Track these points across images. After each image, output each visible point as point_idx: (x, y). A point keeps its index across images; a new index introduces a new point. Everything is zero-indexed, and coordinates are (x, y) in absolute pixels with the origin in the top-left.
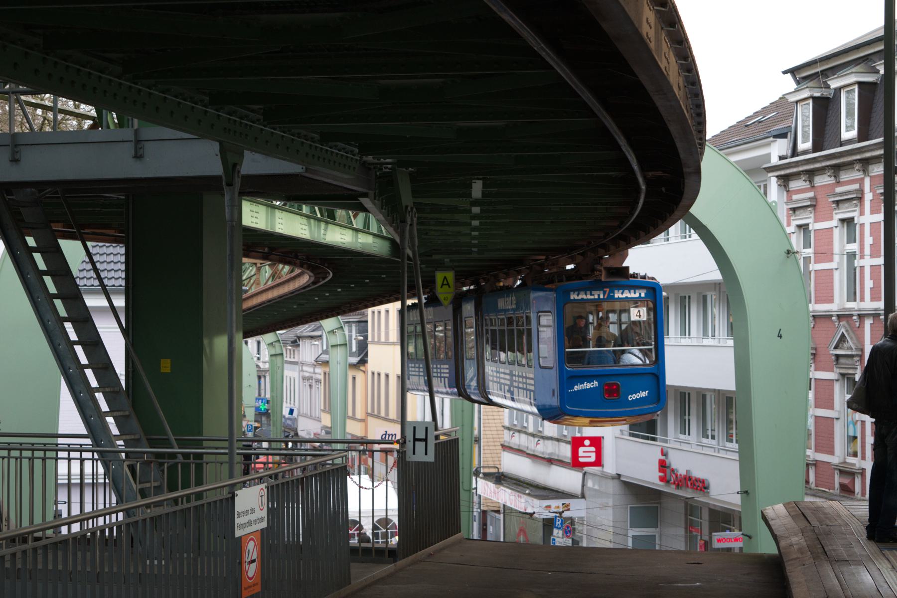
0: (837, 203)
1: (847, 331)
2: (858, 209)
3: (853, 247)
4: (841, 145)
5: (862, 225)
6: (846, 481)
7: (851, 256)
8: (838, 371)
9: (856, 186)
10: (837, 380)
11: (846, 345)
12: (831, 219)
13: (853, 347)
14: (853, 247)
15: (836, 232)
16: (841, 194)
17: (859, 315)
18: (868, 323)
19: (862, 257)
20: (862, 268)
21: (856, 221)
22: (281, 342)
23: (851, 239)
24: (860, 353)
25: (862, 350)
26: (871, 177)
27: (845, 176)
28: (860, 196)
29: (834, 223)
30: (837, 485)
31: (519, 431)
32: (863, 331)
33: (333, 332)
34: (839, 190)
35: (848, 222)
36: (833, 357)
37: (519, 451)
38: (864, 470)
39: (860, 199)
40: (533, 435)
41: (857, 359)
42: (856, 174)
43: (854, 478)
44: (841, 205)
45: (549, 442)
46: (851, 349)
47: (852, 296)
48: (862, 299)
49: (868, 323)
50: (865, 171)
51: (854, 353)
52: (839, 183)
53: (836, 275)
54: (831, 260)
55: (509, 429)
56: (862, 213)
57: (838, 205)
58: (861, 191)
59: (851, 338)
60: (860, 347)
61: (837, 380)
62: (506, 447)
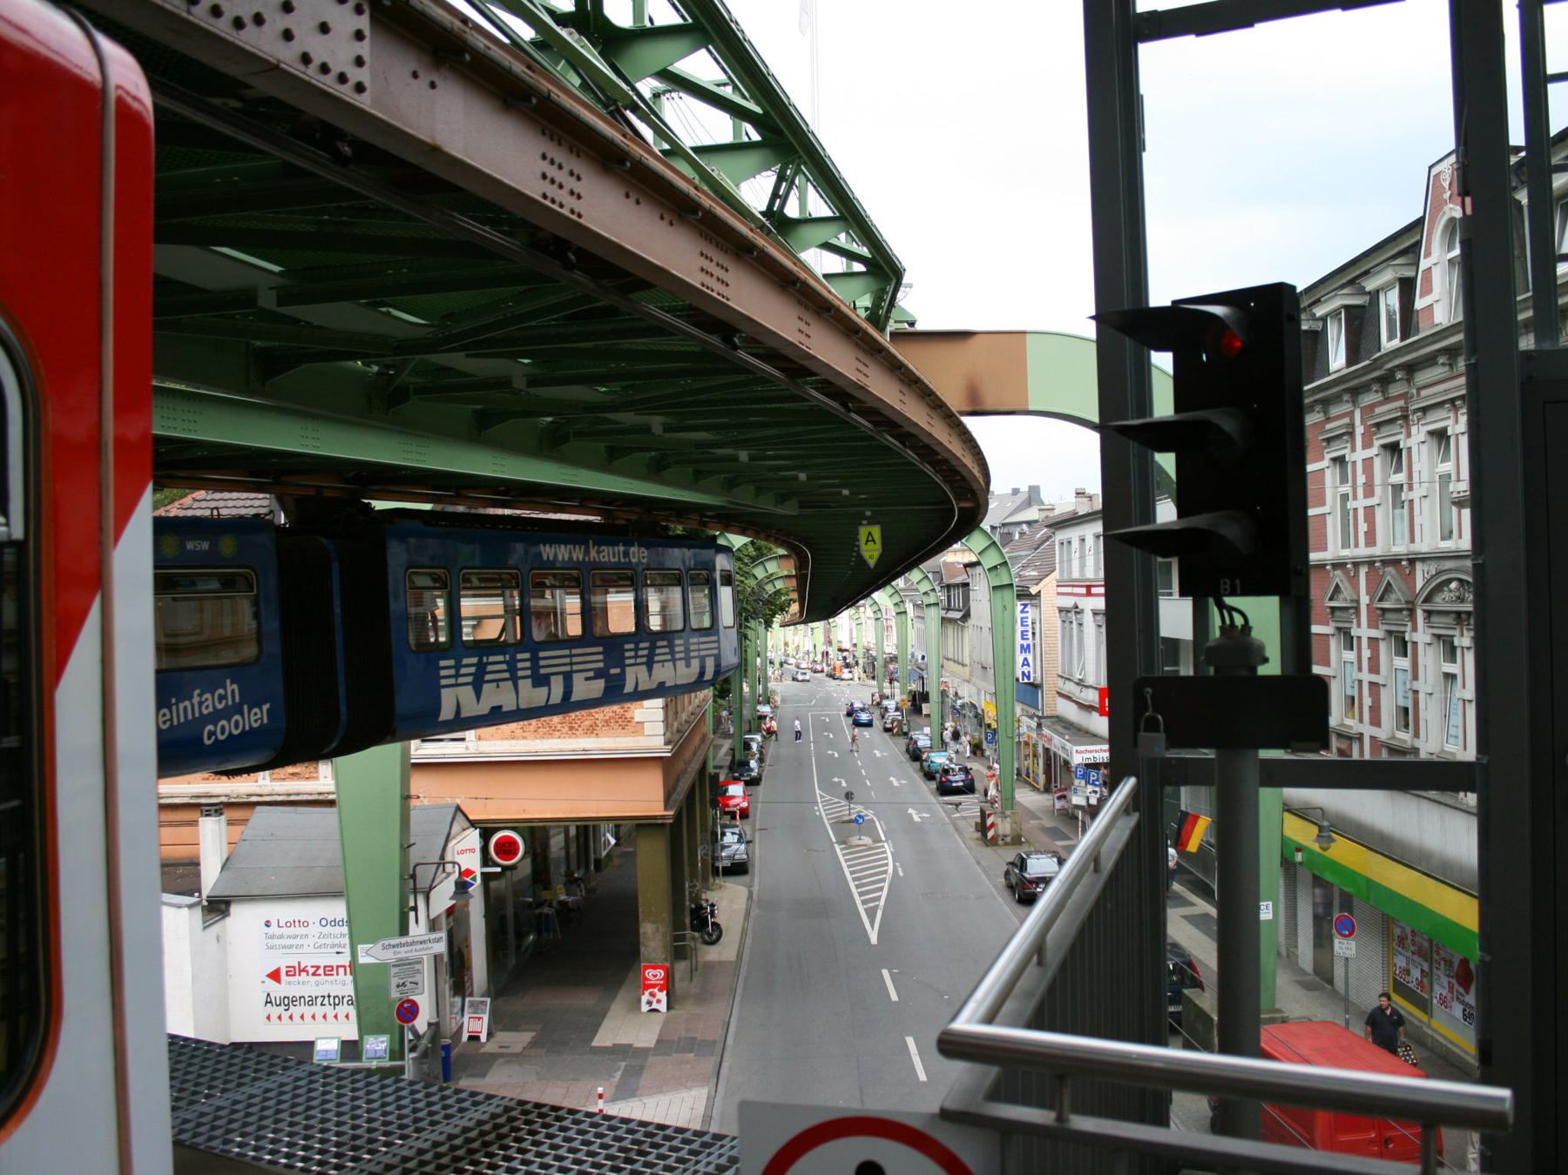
0: (1328, 440)
1: (1341, 581)
2: (1349, 445)
3: (1346, 489)
4: (1329, 375)
5: (1354, 463)
6: (1343, 746)
7: (1345, 497)
8: (1333, 624)
9: (1347, 420)
10: (1333, 635)
11: (1341, 596)
12: (1322, 459)
13: (1349, 598)
14: (1346, 489)
15: (1328, 473)
16: (1331, 430)
17: (1354, 563)
18: (1363, 571)
19: (1355, 498)
20: (1356, 510)
21: (1347, 459)
22: (1015, 589)
23: (1344, 480)
24: (1355, 605)
25: (1358, 601)
26: (1361, 408)
27: (1335, 411)
28: (1351, 430)
29: (1325, 463)
30: (1334, 749)
31: (1069, 679)
32: (1358, 580)
33: (925, 593)
34: (1328, 426)
35: (1340, 461)
36: (1328, 610)
37: (1068, 698)
38: (1362, 734)
39: (1351, 434)
40: (1078, 684)
41: (1352, 611)
42: (1347, 407)
43: (1351, 744)
44: (1332, 444)
45: (1090, 690)
46: (1345, 600)
47: (1345, 545)
48: (1357, 545)
49: (1363, 571)
50: (1354, 403)
51: (1349, 605)
52: (1328, 420)
53: (1329, 519)
54: (1323, 504)
55: (1062, 677)
56: (1353, 450)
57: (1328, 443)
58: (1352, 425)
59: (1346, 589)
60: (1355, 597)
61: (1333, 635)
62: (1060, 694)
